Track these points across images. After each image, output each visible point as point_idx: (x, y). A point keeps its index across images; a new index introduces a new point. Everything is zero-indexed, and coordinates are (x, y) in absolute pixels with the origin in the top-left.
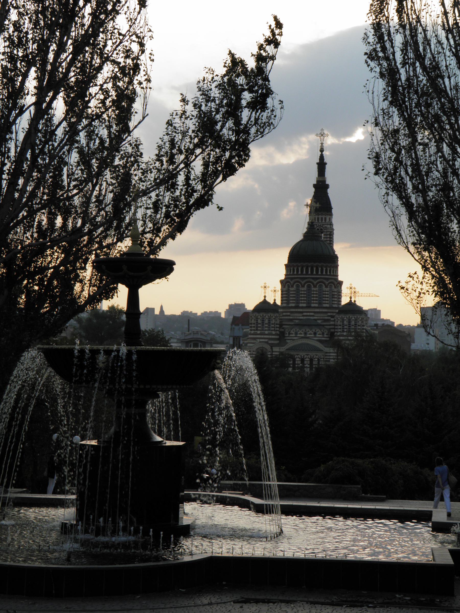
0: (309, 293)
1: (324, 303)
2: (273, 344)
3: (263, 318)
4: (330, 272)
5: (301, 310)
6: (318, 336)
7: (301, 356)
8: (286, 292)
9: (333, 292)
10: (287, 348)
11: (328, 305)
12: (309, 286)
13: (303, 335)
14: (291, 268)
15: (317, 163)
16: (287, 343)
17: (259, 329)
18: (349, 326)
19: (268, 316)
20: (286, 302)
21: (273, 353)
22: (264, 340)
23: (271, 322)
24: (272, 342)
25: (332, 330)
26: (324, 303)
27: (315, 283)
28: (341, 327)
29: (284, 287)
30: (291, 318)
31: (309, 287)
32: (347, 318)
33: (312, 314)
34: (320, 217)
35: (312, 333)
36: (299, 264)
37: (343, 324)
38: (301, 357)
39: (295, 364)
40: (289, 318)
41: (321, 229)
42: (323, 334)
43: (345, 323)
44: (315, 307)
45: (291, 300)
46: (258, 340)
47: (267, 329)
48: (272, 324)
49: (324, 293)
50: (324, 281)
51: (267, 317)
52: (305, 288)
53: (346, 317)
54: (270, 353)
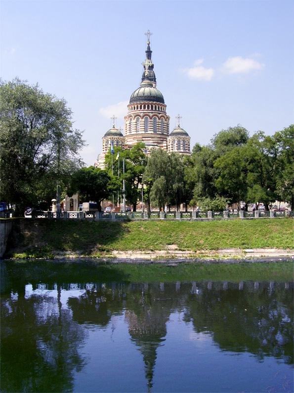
3: (113, 141)
12: (147, 118)
15: (146, 52)
23: (119, 144)
40: (132, 142)
50: (158, 114)
52: (143, 120)
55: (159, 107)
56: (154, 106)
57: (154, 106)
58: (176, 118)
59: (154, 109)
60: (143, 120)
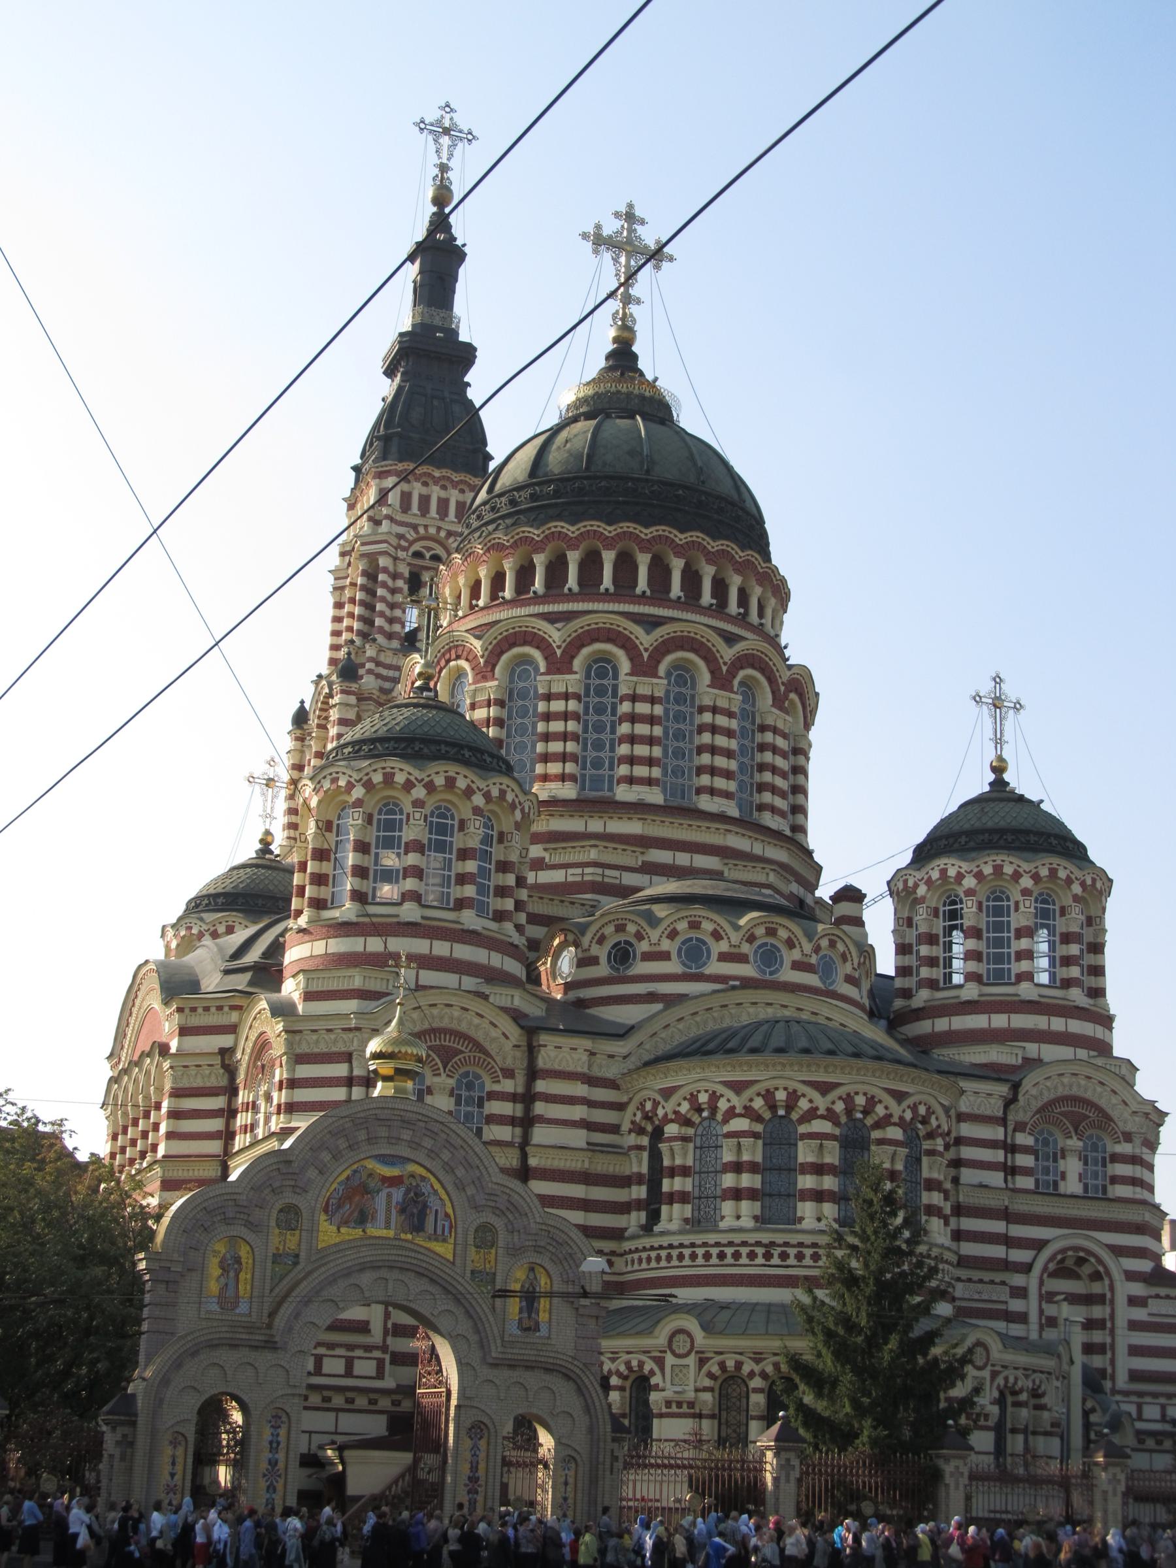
5: (633, 827)
7: (848, 1100)
10: (647, 1057)
14: (540, 560)
21: (541, 1086)
26: (761, 808)
27: (727, 654)
30: (557, 876)
31: (681, 681)
34: (436, 492)
38: (849, 1111)
39: (792, 1169)
44: (721, 818)
49: (769, 737)
51: (478, 800)
54: (508, 1086)
59: (733, 608)
60: (657, 685)
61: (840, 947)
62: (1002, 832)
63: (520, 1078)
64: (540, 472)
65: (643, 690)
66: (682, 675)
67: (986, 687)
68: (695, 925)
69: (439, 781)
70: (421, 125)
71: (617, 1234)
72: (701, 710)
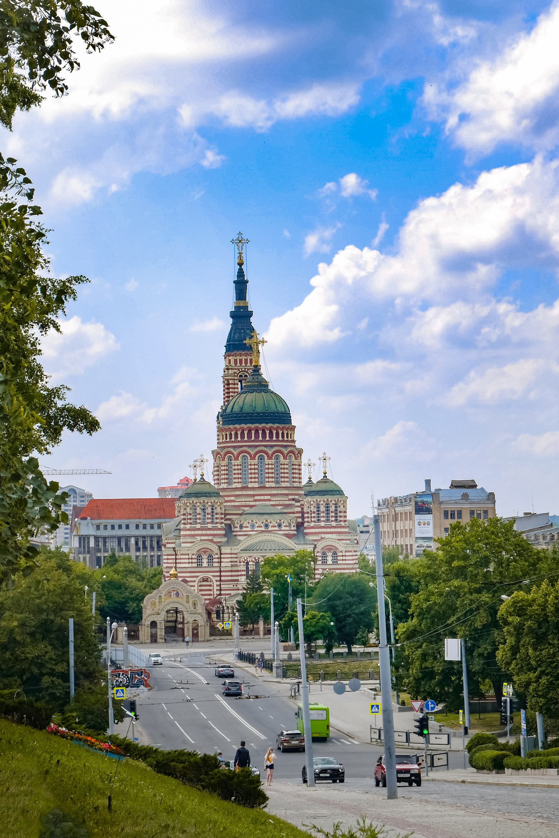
0: (261, 467)
1: (282, 482)
2: (220, 542)
4: (287, 437)
5: (251, 493)
6: (283, 528)
8: (226, 468)
9: (293, 465)
10: (242, 549)
11: (288, 485)
12: (261, 458)
13: (263, 529)
14: (233, 433)
15: (235, 282)
16: (240, 541)
17: (198, 521)
18: (328, 514)
19: (211, 502)
20: (226, 481)
21: (222, 556)
22: (206, 538)
23: (215, 511)
24: (219, 540)
25: (300, 520)
26: (282, 482)
27: (270, 453)
28: (315, 515)
29: (223, 460)
31: (261, 459)
32: (324, 501)
33: (268, 497)
34: (243, 358)
35: (276, 525)
36: (245, 426)
37: (318, 511)
40: (233, 504)
41: (246, 376)
42: (290, 525)
43: (322, 509)
44: (271, 488)
45: (235, 478)
46: (198, 538)
47: (209, 521)
48: (217, 514)
49: (283, 466)
50: (283, 449)
51: (210, 504)
52: (256, 461)
53: (322, 499)
54: (217, 556)
55: (283, 434)
56: (274, 432)
57: (274, 432)
58: (320, 459)
59: (274, 438)
60: (256, 461)
61: (282, 521)
62: (319, 491)
63: (219, 555)
64: (233, 411)
65: (252, 463)
66: (261, 458)
67: (321, 456)
68: (252, 521)
69: (202, 502)
70: (232, 241)
71: (238, 580)
72: (266, 464)
